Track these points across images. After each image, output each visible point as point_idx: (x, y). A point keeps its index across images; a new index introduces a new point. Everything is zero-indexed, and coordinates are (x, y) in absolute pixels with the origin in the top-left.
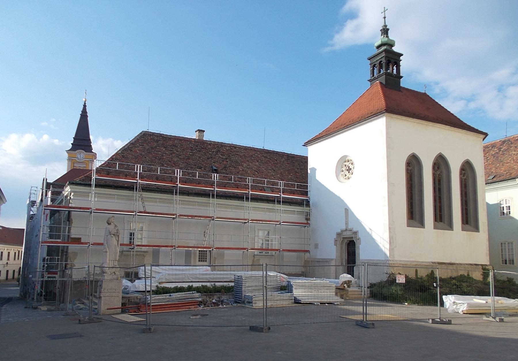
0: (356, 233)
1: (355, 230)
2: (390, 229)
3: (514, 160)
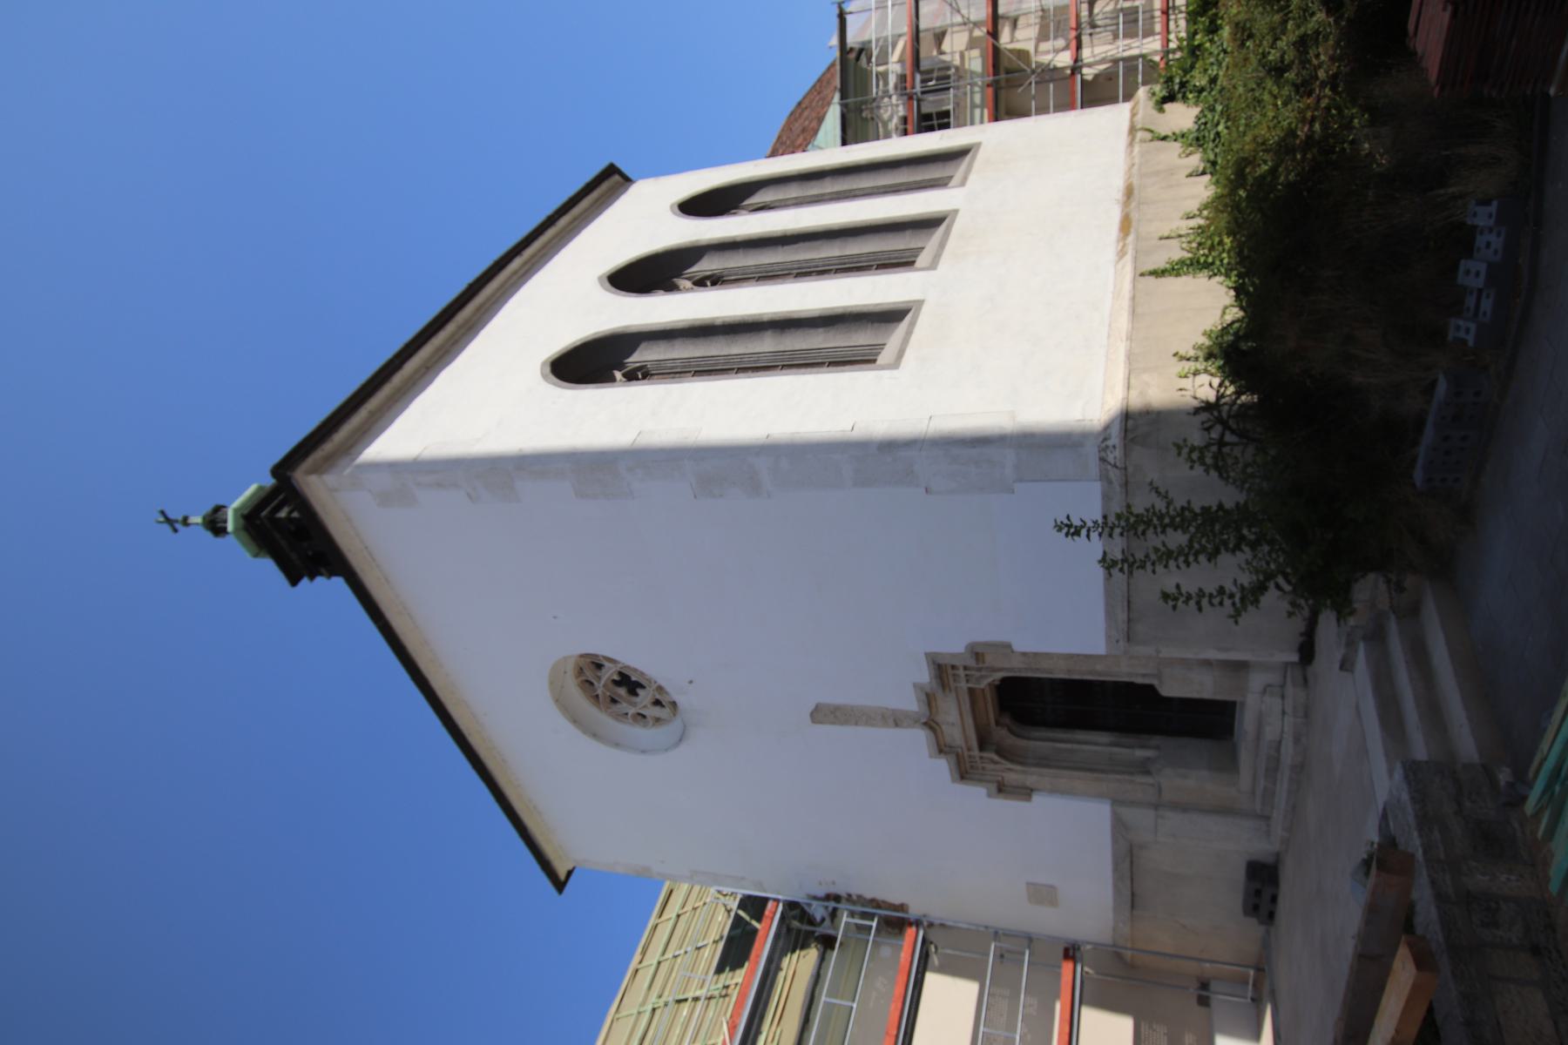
0: (942, 670)
1: (924, 676)
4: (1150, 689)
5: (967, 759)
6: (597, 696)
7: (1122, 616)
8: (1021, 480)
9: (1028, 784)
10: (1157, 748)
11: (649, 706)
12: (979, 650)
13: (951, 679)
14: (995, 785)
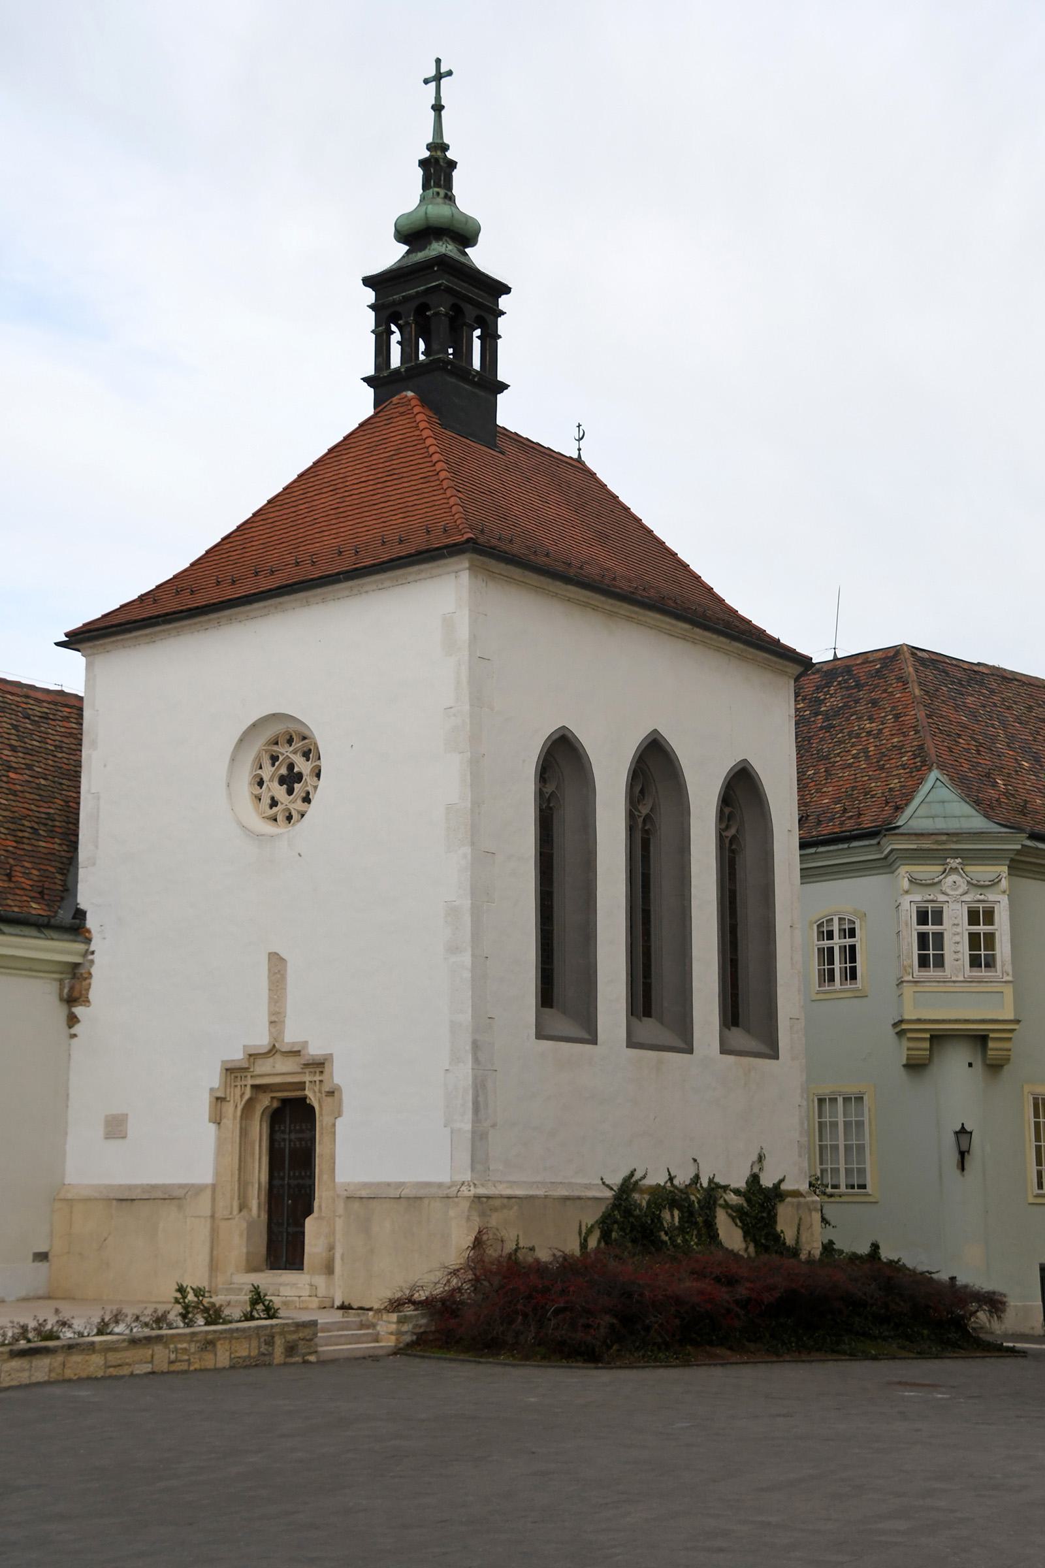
1: (315, 1050)
2: (476, 1046)
3: (867, 757)
4: (309, 1211)
5: (245, 1074)
6: (277, 743)
7: (364, 1193)
8: (452, 1132)
9: (224, 1121)
10: (259, 1216)
11: (270, 794)
12: (336, 1093)
13: (312, 1070)
14: (223, 1096)
